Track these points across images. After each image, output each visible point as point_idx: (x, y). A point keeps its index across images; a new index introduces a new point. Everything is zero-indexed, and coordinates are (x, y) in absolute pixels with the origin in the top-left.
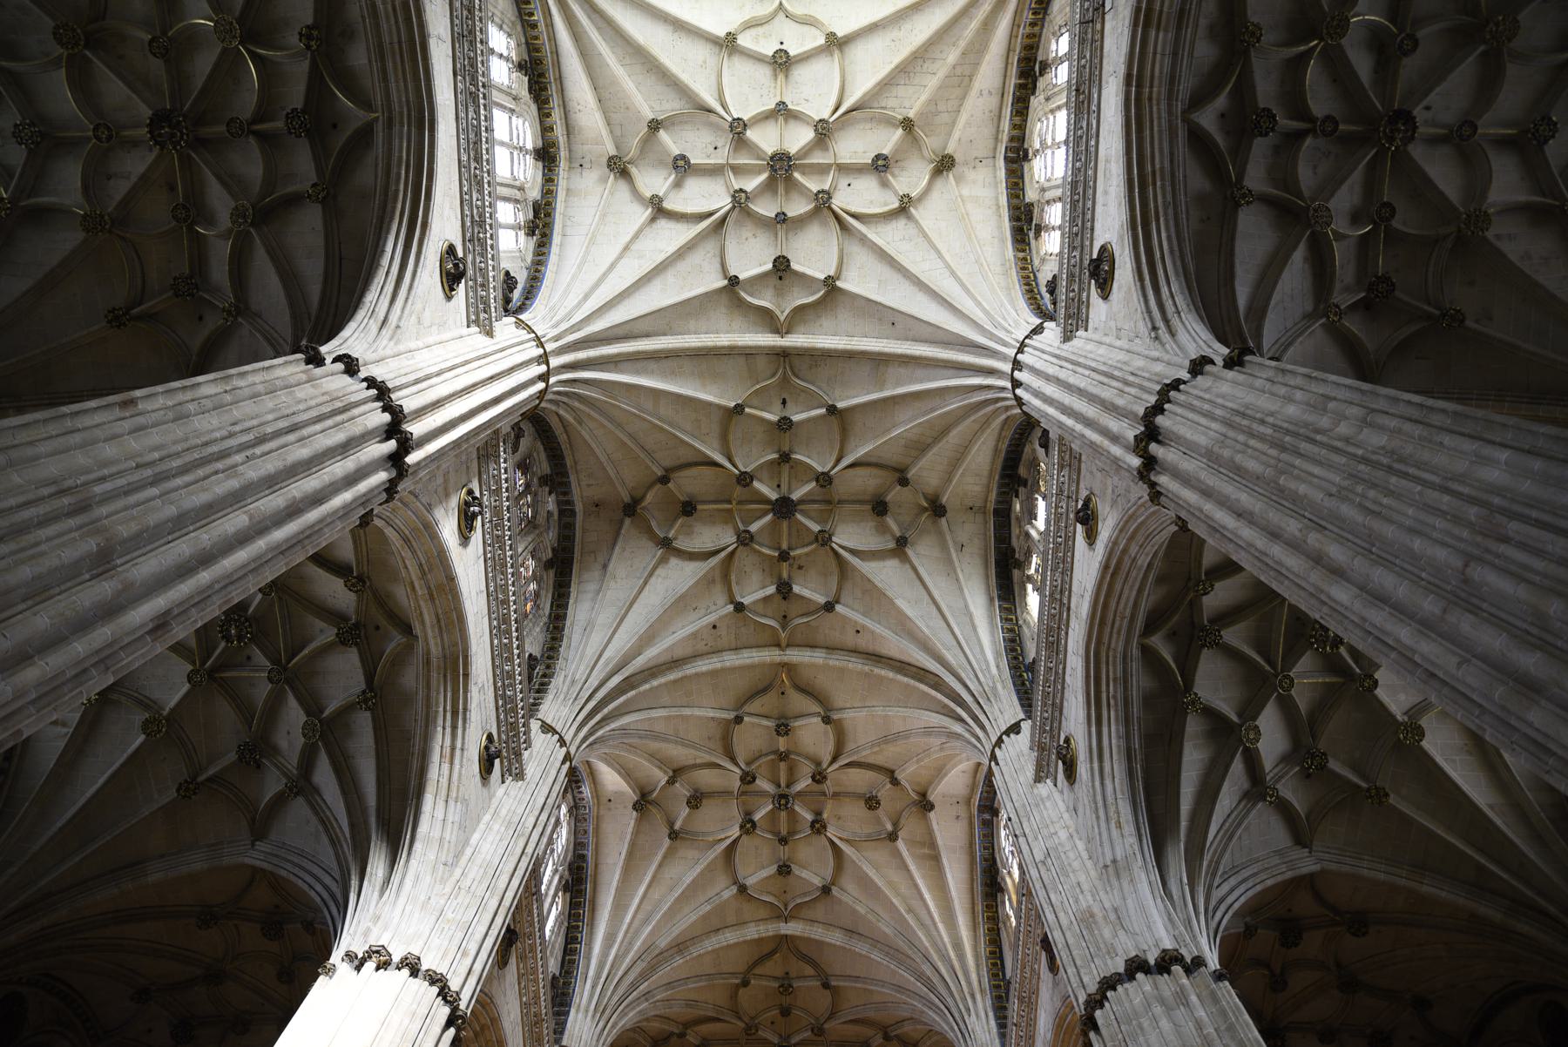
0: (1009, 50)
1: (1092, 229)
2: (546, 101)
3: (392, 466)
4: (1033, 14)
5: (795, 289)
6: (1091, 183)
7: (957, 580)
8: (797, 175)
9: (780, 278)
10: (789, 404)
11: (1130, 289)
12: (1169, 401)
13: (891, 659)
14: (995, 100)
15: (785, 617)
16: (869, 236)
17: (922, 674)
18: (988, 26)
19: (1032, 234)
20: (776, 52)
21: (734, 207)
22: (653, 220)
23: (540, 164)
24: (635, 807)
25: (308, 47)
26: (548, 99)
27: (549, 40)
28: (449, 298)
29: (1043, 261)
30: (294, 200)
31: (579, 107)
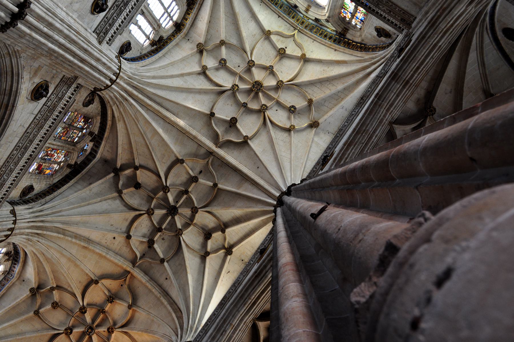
2: (191, 9)
3: (10, 18)
5: (233, 134)
7: (217, 283)
8: (260, 94)
9: (230, 127)
10: (202, 174)
13: (171, 298)
15: (144, 255)
16: (271, 131)
17: (178, 310)
18: (358, 82)
20: (282, 48)
21: (230, 90)
22: (199, 74)
23: (174, 29)
24: (32, 290)
26: (192, 8)
31: (202, 19)
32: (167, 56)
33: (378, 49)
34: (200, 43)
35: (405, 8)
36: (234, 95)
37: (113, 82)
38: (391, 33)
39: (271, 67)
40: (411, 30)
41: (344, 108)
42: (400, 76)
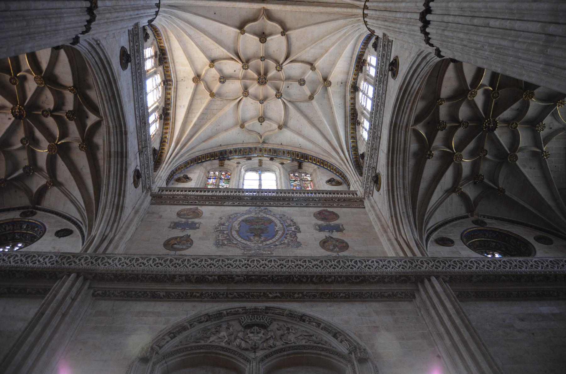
1: (132, 73)
2: (352, 109)
3: (430, 7)
4: (166, 141)
6: (135, 90)
8: (256, 76)
9: (264, 33)
11: (112, 56)
12: (85, 26)
14: (178, 104)
16: (226, 51)
19: (158, 53)
21: (282, 64)
23: (357, 85)
25: (431, 152)
27: (347, 132)
28: (397, 57)
29: (152, 44)
30: (449, 99)
32: (350, 59)
33: (183, 166)
34: (330, 86)
36: (277, 62)
37: (365, 7)
38: (177, 183)
39: (262, 101)
40: (149, 193)
41: (182, 107)
42: (118, 158)
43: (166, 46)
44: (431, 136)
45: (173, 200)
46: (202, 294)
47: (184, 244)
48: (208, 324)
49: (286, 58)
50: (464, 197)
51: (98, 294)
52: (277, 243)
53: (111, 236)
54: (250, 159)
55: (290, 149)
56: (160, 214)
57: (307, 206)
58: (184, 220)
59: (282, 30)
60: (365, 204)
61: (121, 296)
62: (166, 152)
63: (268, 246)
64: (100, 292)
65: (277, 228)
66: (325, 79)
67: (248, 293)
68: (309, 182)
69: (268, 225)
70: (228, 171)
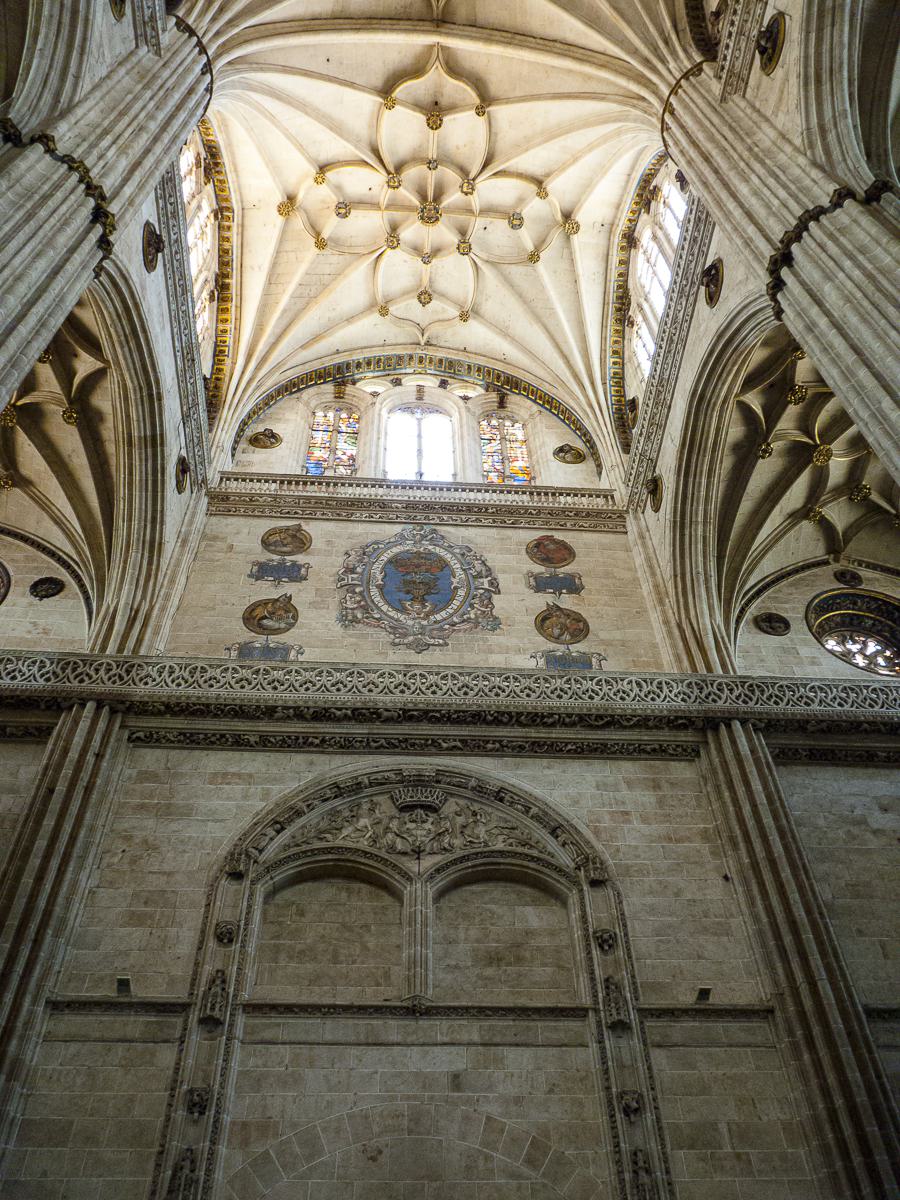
0: (240, 307)
8: (416, 201)
9: (436, 103)
19: (203, 155)
21: (474, 180)
22: (548, 175)
23: (636, 234)
25: (769, 445)
35: (231, 520)
36: (463, 171)
39: (427, 259)
41: (257, 269)
42: (146, 447)
43: (220, 139)
44: (773, 412)
45: (251, 506)
46: (323, 741)
47: (280, 619)
48: (337, 802)
49: (485, 166)
50: (826, 526)
51: (138, 738)
52: (455, 619)
53: (145, 607)
54: (397, 382)
55: (482, 362)
56: (229, 541)
57: (514, 526)
58: (276, 557)
59: (477, 101)
60: (628, 524)
61: (179, 741)
62: (227, 379)
63: (437, 626)
64: (141, 734)
65: (455, 581)
66: (567, 216)
67: (406, 740)
68: (518, 444)
69: (439, 574)
70: (354, 409)
